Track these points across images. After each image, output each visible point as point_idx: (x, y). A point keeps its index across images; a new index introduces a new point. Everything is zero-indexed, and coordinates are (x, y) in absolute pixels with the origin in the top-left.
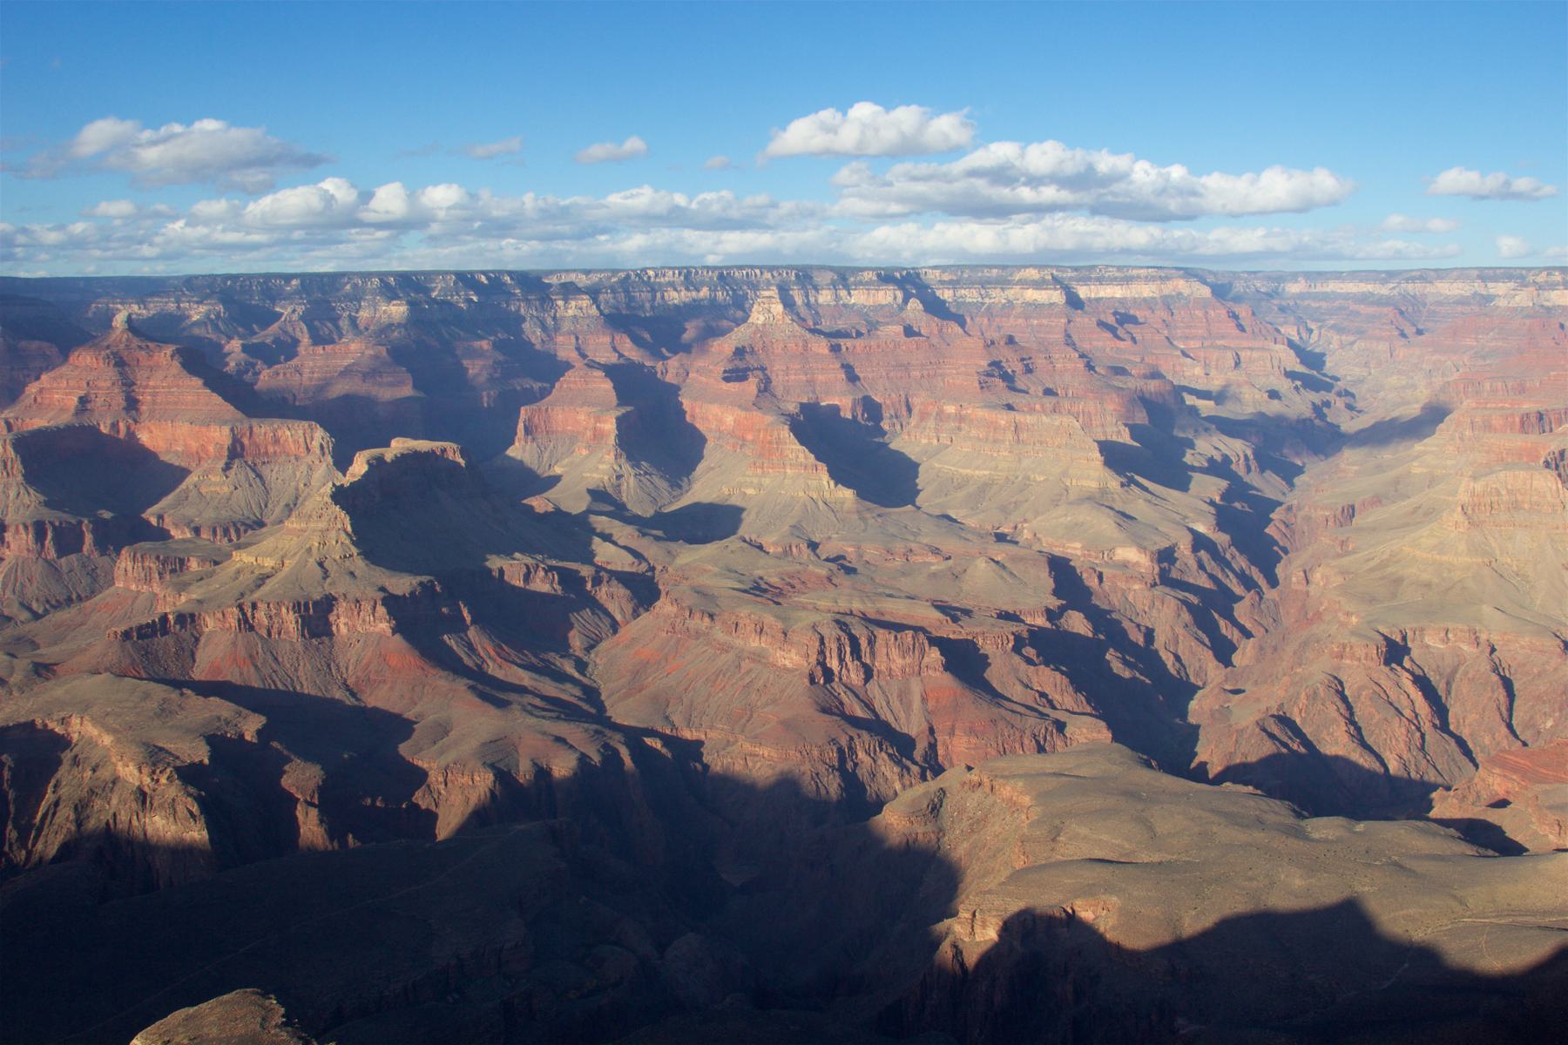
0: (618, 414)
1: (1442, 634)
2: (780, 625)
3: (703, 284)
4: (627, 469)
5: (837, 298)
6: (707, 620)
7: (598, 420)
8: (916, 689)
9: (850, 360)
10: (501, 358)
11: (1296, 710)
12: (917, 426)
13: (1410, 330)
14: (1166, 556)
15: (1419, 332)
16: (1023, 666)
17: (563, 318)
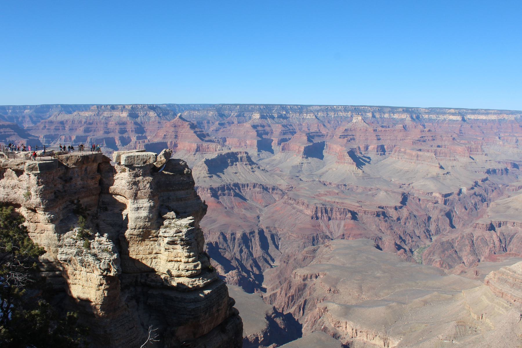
0: (305, 146)
3: (350, 110)
4: (305, 161)
7: (300, 147)
16: (378, 221)
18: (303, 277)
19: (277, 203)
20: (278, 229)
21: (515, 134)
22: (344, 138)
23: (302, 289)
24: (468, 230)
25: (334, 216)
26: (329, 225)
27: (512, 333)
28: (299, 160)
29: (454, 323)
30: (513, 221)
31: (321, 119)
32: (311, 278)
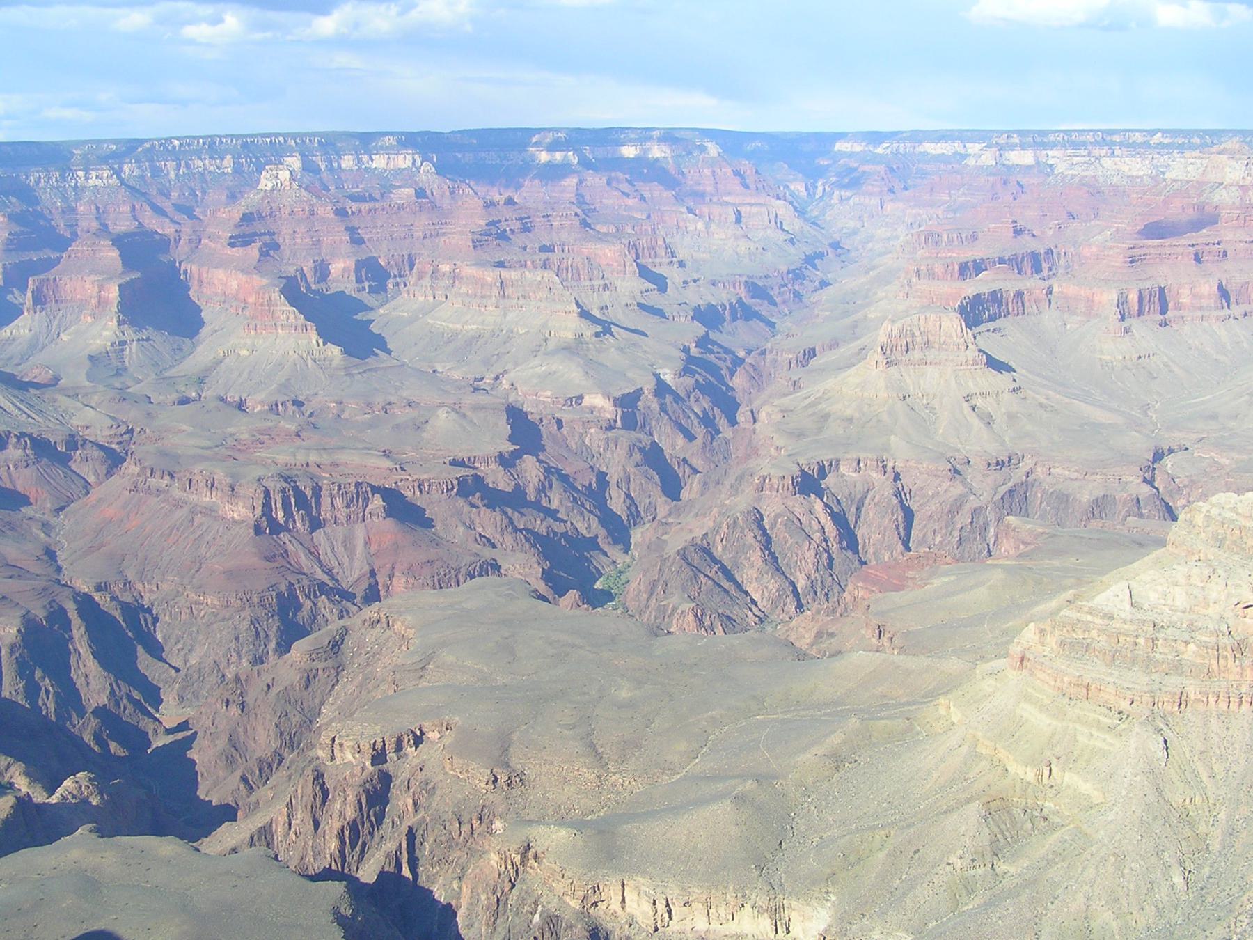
0: (122, 281)
1: (855, 464)
2: (229, 480)
3: (227, 152)
4: (130, 334)
5: (359, 161)
6: (167, 477)
7: (101, 288)
8: (360, 532)
9: (355, 222)
10: (17, 229)
11: (718, 539)
12: (415, 285)
13: (898, 186)
14: (628, 402)
15: (905, 188)
16: (467, 508)
17: (84, 188)
18: (368, 753)
19: (95, 494)
20: (139, 587)
21: (727, 199)
22: (246, 244)
23: (377, 795)
24: (742, 502)
25: (325, 512)
26: (316, 547)
27: (1162, 801)
28: (106, 333)
29: (974, 809)
30: (854, 455)
31: (132, 183)
32: (399, 747)
